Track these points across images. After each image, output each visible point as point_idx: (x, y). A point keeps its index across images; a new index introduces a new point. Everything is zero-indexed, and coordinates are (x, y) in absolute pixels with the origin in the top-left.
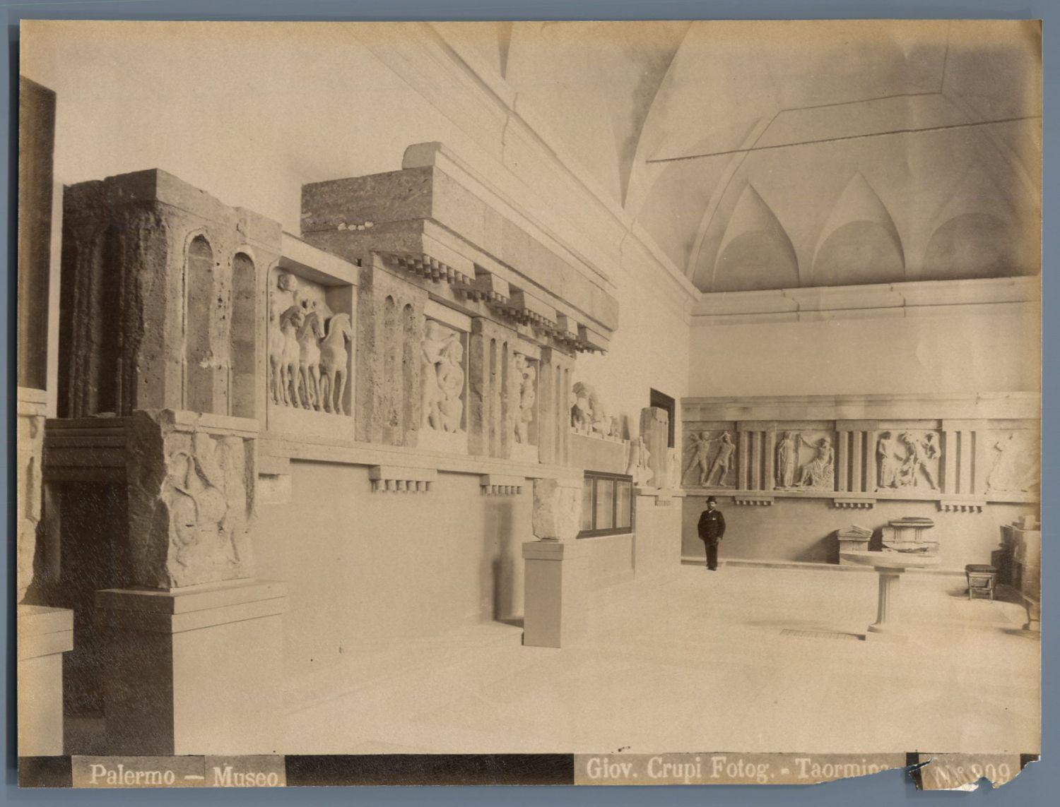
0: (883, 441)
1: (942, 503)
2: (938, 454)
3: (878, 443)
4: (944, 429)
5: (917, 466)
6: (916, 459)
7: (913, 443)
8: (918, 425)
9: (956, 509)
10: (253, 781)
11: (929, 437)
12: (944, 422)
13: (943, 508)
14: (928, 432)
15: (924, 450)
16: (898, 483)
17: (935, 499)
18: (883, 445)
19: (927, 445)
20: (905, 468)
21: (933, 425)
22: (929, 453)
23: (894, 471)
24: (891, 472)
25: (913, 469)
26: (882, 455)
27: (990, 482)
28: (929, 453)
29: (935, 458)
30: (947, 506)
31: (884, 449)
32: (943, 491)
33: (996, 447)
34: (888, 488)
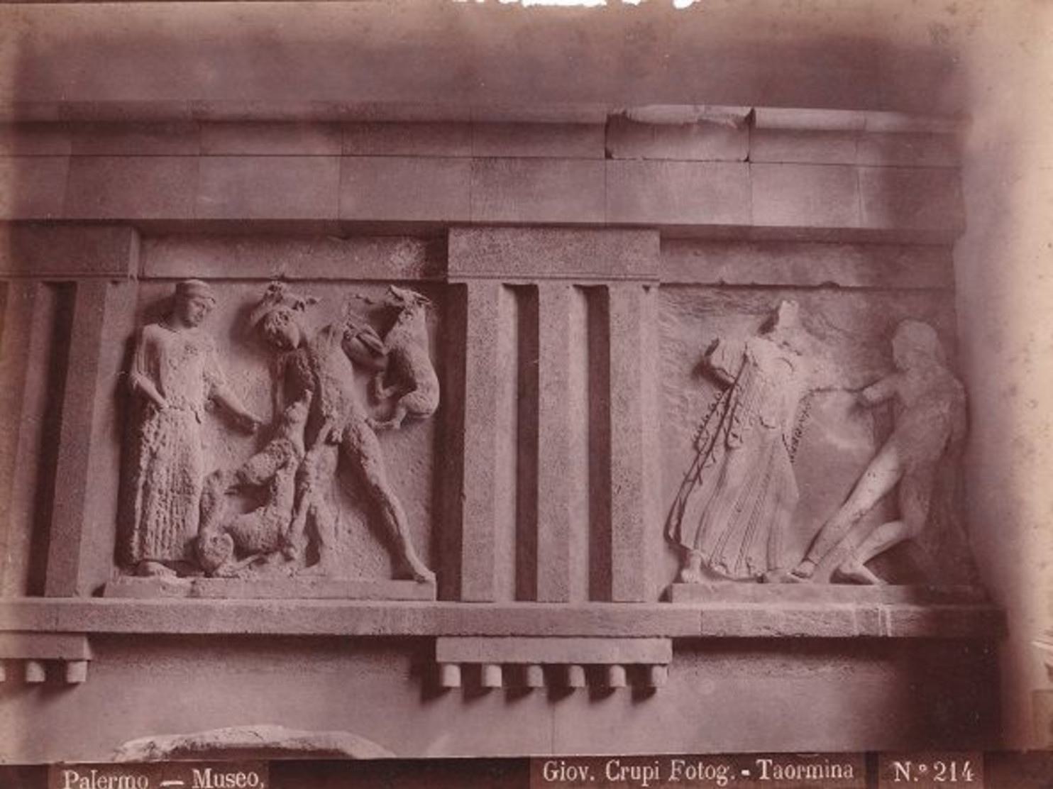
0: (154, 331)
1: (444, 650)
2: (428, 397)
3: (131, 344)
4: (456, 270)
5: (323, 459)
6: (315, 421)
7: (303, 343)
8: (330, 263)
9: (515, 676)
10: (228, 780)
11: (387, 317)
12: (458, 243)
13: (453, 677)
14: (378, 296)
15: (364, 381)
16: (216, 544)
17: (406, 627)
18: (154, 349)
19: (374, 352)
20: (262, 465)
21: (403, 260)
22: (384, 393)
23: (199, 483)
24: (187, 488)
25: (301, 476)
26: (145, 398)
27: (687, 541)
28: (384, 393)
29: (413, 417)
30: (472, 672)
31: (156, 375)
32: (449, 587)
33: (704, 371)
34: (170, 577)
